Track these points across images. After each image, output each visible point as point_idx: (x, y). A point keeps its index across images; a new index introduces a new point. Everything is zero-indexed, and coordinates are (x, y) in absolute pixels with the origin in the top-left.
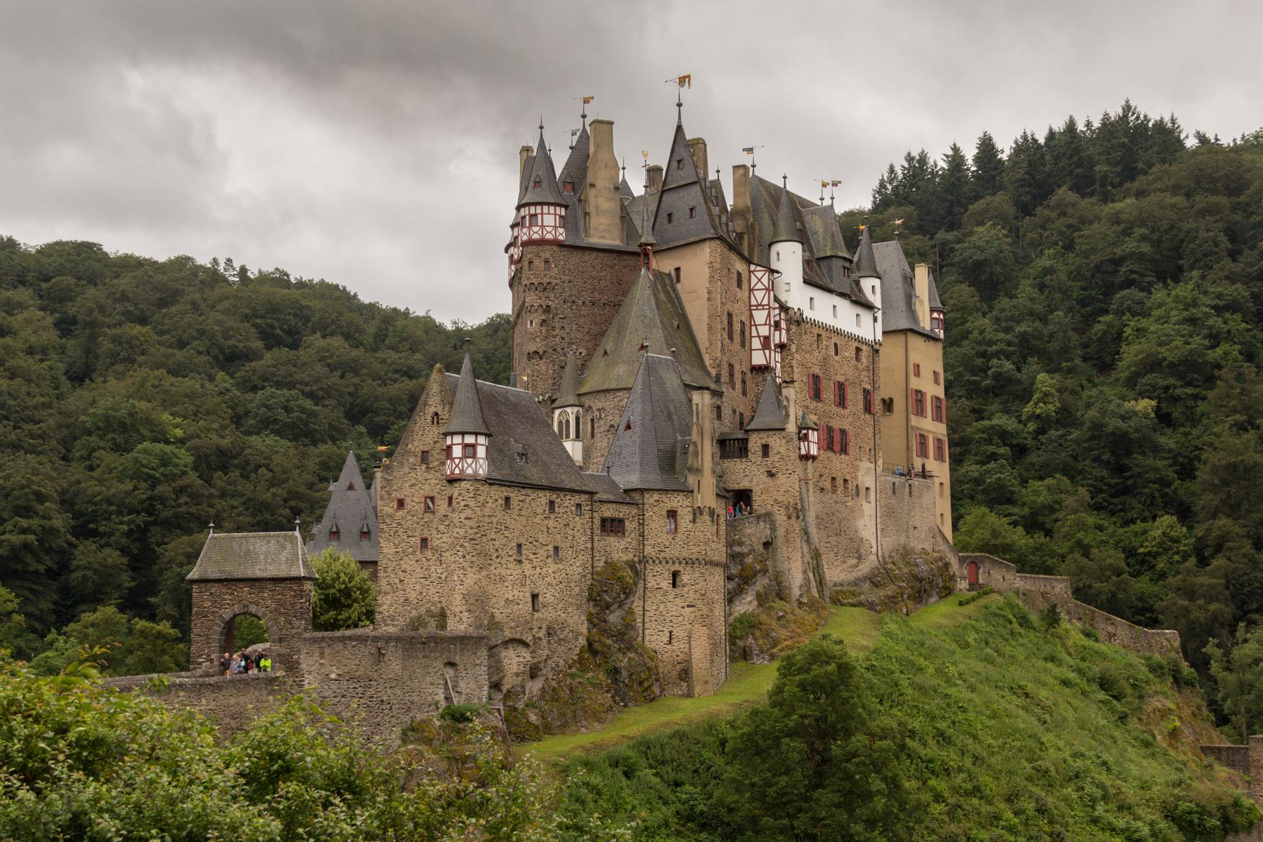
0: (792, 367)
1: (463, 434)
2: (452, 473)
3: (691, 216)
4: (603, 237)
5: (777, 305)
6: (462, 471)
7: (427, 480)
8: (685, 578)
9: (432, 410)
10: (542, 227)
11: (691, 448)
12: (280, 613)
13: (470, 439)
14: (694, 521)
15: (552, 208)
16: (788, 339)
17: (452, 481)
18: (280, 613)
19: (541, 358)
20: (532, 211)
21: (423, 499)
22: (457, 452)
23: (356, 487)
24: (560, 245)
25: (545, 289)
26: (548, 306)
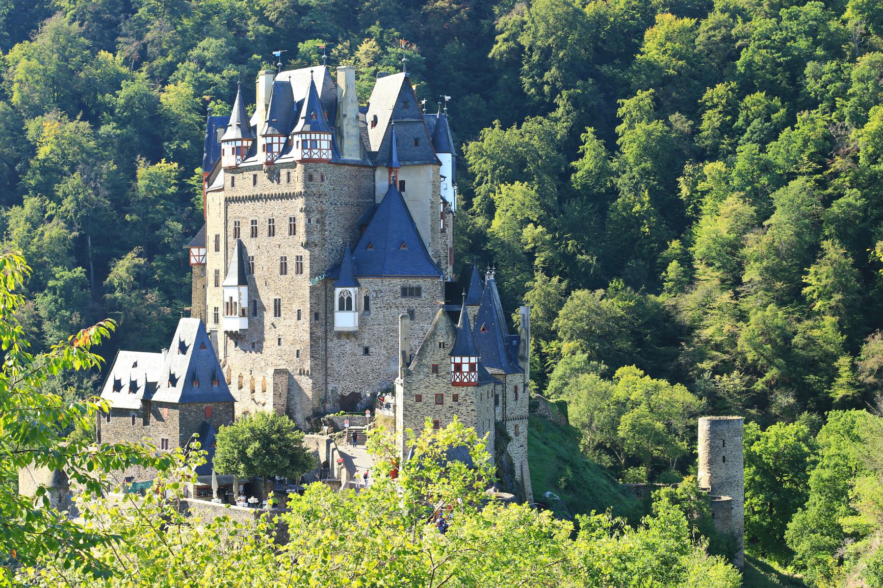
3: (416, 144)
4: (350, 155)
8: (520, 428)
10: (320, 149)
11: (522, 344)
17: (455, 384)
19: (316, 245)
22: (465, 368)
24: (329, 162)
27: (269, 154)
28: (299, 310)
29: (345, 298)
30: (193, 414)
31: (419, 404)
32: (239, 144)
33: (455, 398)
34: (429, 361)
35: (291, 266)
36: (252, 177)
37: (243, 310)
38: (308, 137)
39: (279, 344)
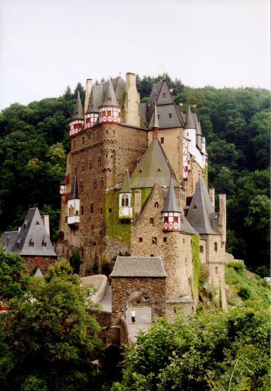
0: (193, 179)
1: (173, 212)
2: (168, 228)
5: (189, 154)
6: (173, 228)
7: (153, 230)
9: (155, 201)
10: (113, 116)
11: (220, 218)
12: (157, 292)
13: (176, 215)
14: (222, 247)
15: (116, 109)
16: (192, 168)
17: (166, 231)
18: (155, 292)
19: (110, 171)
20: (109, 110)
21: (151, 238)
22: (171, 219)
23: (40, 223)
24: (119, 125)
25: (113, 143)
26: (114, 150)
27: (89, 124)
28: (102, 208)
29: (125, 199)
30: (29, 262)
31: (141, 243)
32: (77, 122)
33: (165, 240)
34: (147, 215)
35: (99, 183)
36: (82, 139)
37: (77, 212)
38: (106, 110)
39: (92, 228)
